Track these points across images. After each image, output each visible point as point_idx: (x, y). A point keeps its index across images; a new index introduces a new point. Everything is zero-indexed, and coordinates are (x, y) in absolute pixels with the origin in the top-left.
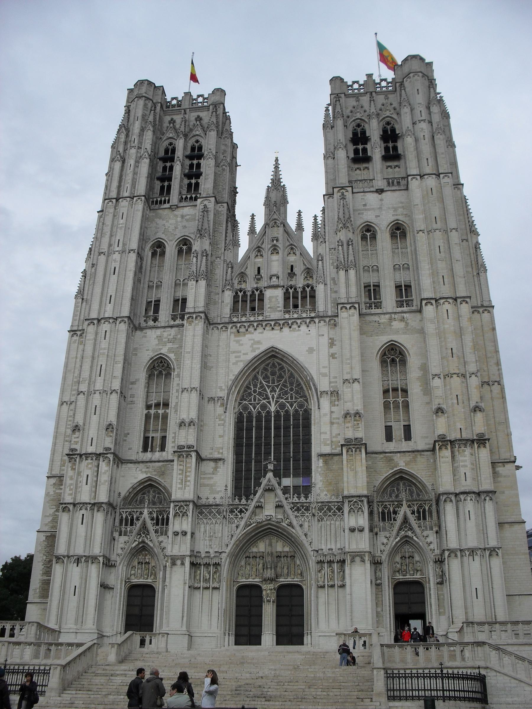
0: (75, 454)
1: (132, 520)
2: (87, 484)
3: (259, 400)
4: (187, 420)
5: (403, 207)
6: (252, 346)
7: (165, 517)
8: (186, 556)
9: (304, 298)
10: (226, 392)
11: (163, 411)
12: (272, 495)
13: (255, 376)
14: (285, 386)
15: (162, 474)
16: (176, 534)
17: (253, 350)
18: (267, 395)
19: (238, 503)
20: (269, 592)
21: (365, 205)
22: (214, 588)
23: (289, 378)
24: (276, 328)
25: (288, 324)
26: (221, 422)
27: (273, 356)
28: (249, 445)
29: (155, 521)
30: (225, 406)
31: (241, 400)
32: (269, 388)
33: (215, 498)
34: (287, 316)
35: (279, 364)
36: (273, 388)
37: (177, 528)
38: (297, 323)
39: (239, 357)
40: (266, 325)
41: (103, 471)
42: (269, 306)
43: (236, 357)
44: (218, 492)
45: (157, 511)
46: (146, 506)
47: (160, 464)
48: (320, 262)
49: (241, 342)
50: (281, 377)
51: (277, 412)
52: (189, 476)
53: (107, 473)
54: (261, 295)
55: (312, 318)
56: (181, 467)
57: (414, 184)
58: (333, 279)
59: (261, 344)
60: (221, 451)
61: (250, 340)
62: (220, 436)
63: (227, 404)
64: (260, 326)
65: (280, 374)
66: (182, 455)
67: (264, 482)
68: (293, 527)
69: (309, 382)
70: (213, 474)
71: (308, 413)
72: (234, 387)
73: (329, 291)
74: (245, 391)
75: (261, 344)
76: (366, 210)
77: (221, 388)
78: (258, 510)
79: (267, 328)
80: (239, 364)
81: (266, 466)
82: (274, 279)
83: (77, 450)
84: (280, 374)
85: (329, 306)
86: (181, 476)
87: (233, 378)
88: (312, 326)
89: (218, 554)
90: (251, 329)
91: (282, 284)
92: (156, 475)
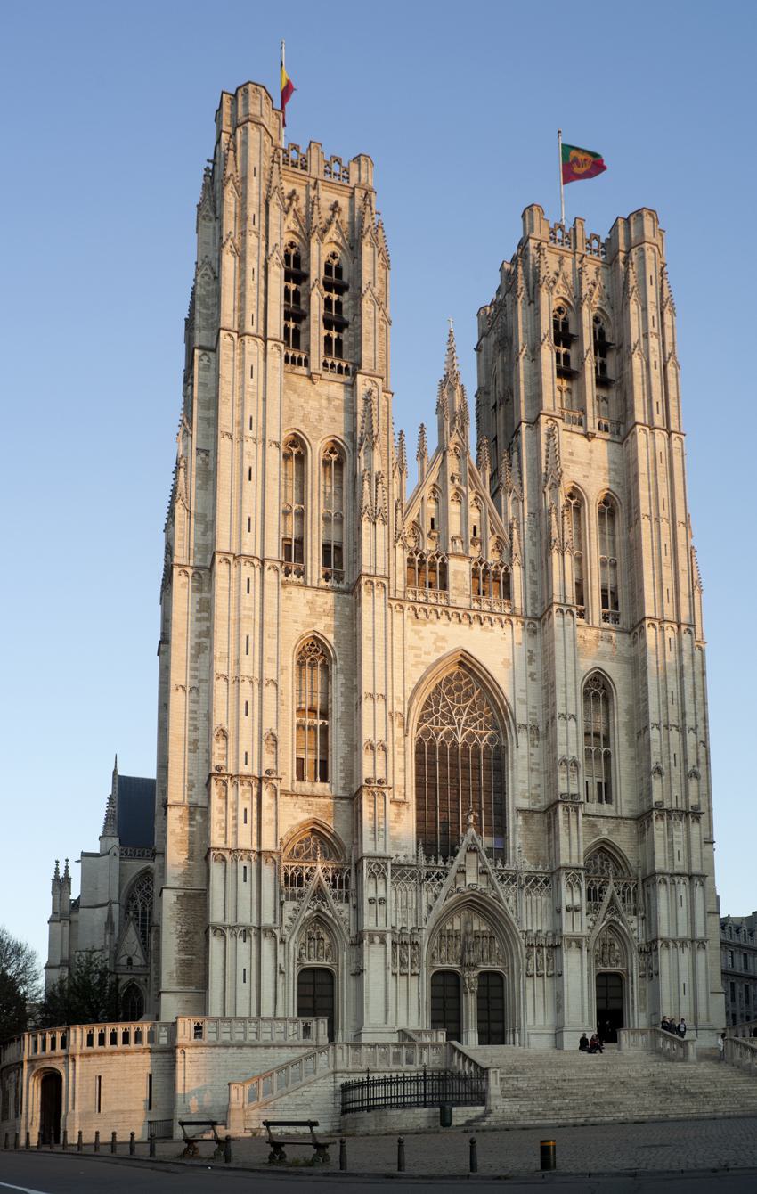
1: (300, 878)
6: (434, 643)
7: (344, 877)
10: (406, 706)
12: (474, 856)
13: (436, 687)
17: (437, 650)
19: (435, 865)
21: (571, 454)
29: (331, 883)
30: (405, 725)
34: (476, 606)
42: (454, 585)
43: (416, 656)
48: (515, 532)
49: (421, 635)
54: (444, 567)
55: (508, 615)
57: (641, 437)
58: (532, 562)
59: (446, 642)
61: (432, 633)
63: (408, 725)
67: (466, 840)
70: (396, 822)
72: (415, 702)
73: (528, 580)
74: (425, 708)
75: (446, 642)
76: (573, 462)
78: (460, 876)
80: (420, 666)
82: (458, 543)
85: (529, 601)
87: (413, 687)
91: (471, 555)
92: (321, 816)
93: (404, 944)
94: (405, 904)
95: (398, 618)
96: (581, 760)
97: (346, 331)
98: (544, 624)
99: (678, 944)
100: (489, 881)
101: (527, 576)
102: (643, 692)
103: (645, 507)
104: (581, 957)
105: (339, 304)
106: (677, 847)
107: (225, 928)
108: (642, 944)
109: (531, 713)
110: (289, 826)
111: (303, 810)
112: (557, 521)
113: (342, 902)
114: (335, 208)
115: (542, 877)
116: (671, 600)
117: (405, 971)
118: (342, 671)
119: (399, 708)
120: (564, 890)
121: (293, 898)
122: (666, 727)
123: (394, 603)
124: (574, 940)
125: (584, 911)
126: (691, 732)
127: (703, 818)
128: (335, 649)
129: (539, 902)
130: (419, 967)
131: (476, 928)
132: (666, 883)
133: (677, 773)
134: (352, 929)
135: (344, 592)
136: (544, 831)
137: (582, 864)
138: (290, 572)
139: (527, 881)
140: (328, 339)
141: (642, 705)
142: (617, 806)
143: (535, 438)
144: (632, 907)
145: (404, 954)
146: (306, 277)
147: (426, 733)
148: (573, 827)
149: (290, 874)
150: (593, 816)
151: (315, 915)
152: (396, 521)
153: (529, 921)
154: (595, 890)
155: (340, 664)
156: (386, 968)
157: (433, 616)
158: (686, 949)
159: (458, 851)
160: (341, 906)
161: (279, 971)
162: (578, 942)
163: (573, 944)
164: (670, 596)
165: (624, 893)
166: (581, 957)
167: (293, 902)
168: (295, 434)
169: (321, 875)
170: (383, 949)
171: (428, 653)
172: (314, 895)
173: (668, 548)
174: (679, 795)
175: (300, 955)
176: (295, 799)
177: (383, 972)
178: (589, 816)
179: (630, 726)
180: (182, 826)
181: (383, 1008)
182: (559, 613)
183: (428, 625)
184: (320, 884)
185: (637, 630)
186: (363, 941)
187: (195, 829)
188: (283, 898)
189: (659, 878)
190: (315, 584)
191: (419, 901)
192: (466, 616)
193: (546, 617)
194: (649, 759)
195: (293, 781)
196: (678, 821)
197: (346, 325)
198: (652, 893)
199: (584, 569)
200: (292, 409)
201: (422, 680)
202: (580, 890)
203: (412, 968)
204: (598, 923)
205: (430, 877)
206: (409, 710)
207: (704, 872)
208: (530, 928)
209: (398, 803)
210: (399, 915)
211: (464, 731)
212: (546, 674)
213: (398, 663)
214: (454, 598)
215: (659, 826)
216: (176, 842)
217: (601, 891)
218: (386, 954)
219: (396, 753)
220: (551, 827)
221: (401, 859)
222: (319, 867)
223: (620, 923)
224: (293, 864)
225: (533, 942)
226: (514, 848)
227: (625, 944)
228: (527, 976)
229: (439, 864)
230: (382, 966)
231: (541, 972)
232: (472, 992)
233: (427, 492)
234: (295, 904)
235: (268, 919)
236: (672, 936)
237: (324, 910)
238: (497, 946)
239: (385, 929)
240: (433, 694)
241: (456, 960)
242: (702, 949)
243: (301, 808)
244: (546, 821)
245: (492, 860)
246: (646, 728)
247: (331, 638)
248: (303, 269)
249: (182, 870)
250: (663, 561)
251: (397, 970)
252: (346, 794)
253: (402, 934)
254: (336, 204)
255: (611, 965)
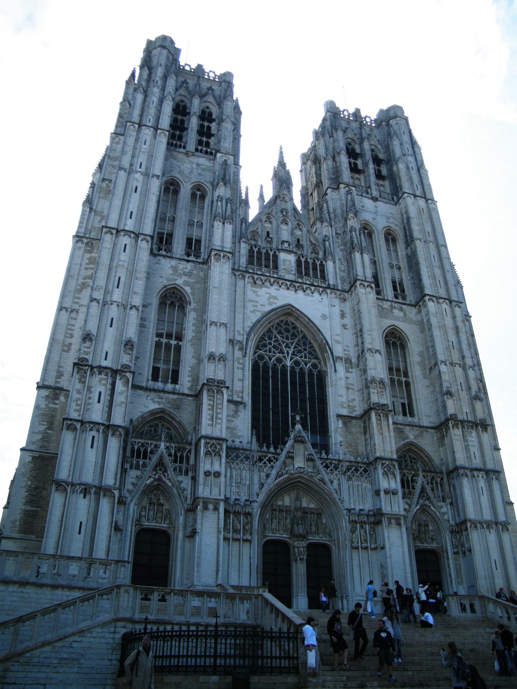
0: (86, 365)
1: (145, 452)
2: (99, 401)
3: (274, 352)
4: (217, 355)
5: (393, 218)
6: (269, 299)
7: (185, 455)
8: (221, 500)
9: (315, 269)
10: (245, 337)
11: (175, 342)
13: (269, 329)
14: (299, 345)
15: (178, 407)
16: (207, 474)
17: (270, 304)
18: (281, 350)
19: (266, 450)
20: (302, 549)
22: (244, 540)
23: (302, 338)
24: (291, 288)
25: (303, 288)
26: (239, 366)
27: (289, 314)
28: (266, 395)
30: (243, 349)
31: (256, 349)
32: (283, 343)
33: (241, 442)
35: (292, 324)
36: (287, 344)
37: (208, 467)
38: (310, 289)
39: (257, 306)
40: (282, 284)
41: (119, 391)
44: (239, 437)
45: (175, 447)
46: (163, 439)
47: (176, 397)
48: (327, 243)
49: (258, 293)
50: (294, 336)
51: (292, 368)
52: (220, 414)
53: (124, 394)
56: (211, 403)
57: (410, 201)
58: (340, 259)
59: (278, 299)
60: (241, 395)
61: (266, 293)
62: (239, 380)
63: (246, 349)
64: (276, 283)
65: (294, 333)
66: (212, 389)
68: (325, 484)
69: (325, 346)
70: (234, 417)
71: (322, 376)
73: (338, 269)
74: (260, 341)
75: (278, 299)
77: (239, 332)
79: (283, 287)
81: (293, 418)
83: (87, 360)
84: (294, 333)
85: (339, 281)
86: (211, 412)
87: (251, 325)
88: (324, 296)
89: (248, 503)
90: (267, 284)
93: (237, 514)
94: (239, 480)
95: (240, 283)
96: (387, 381)
97: (212, 138)
98: (351, 295)
99: (485, 526)
100: (314, 467)
101: (337, 267)
102: (431, 341)
103: (416, 234)
104: (401, 533)
105: (209, 128)
106: (472, 450)
107: (68, 485)
108: (452, 526)
109: (344, 350)
110: (141, 412)
111: (154, 402)
112: (356, 236)
113: (181, 474)
114: (210, 89)
115: (361, 467)
116: (442, 286)
117: (237, 536)
118: (194, 310)
119: (238, 338)
120: (381, 477)
121: (137, 468)
122: (451, 364)
123: (237, 273)
124: (393, 518)
125: (400, 494)
126: (471, 369)
127: (489, 428)
128: (191, 296)
129: (360, 487)
130: (251, 534)
131: (304, 505)
132: (467, 476)
133: (464, 395)
134: (189, 497)
135: (200, 263)
136: (361, 433)
137: (395, 457)
138: (161, 250)
139: (348, 469)
140: (200, 143)
141: (430, 350)
142: (419, 419)
143: (338, 197)
144: (441, 495)
145: (236, 522)
146: (189, 114)
147: (261, 357)
148: (385, 429)
149: (136, 448)
150: (401, 424)
151: (156, 483)
152: (241, 228)
153: (352, 502)
154: (408, 480)
155: (193, 306)
156: (219, 532)
157: (267, 284)
158: (492, 530)
159: (287, 442)
160: (180, 478)
161: (117, 528)
162: (397, 520)
163: (393, 521)
164: (442, 285)
165: (432, 484)
166: (401, 533)
167: (136, 471)
168: (173, 179)
169: (165, 451)
170: (216, 516)
171: (264, 305)
172: (156, 466)
173: (436, 258)
174: (468, 411)
175: (140, 516)
176: (148, 393)
177: (216, 535)
178: (397, 424)
179: (422, 364)
180: (47, 403)
181: (214, 568)
182: (362, 286)
183: (263, 289)
184: (161, 458)
185: (421, 304)
186: (197, 507)
187: (57, 406)
188: (127, 466)
189: (461, 471)
190: (178, 256)
191: (251, 478)
192: (292, 285)
193: (353, 289)
194: (441, 385)
195: (148, 380)
196: (470, 430)
197: (213, 135)
198: (456, 483)
199: (378, 267)
200: (171, 167)
201: (258, 321)
202: (395, 477)
203: (244, 534)
204: (413, 506)
205: (263, 460)
206: (247, 340)
207: (497, 469)
208: (353, 507)
209: (237, 403)
210: (234, 489)
211: (291, 359)
212: (356, 324)
213: (239, 309)
214: (283, 274)
215: (456, 434)
216: (39, 415)
217: (413, 481)
218: (219, 519)
219: (235, 368)
220: (366, 430)
221: (237, 444)
222: (163, 445)
223: (432, 507)
224: (140, 441)
225: (356, 518)
226: (335, 444)
227: (437, 524)
228: (352, 548)
229: (270, 451)
230: (215, 531)
231: (364, 545)
232: (302, 559)
233: (264, 218)
234: (138, 473)
235: (109, 480)
236: (478, 518)
237: (164, 479)
238: (324, 521)
239: (219, 498)
240: (267, 332)
241: (285, 531)
242: (506, 531)
243: (152, 400)
244: (362, 425)
245: (317, 450)
246: (436, 364)
247: (188, 289)
248: (188, 111)
249: (40, 436)
250: (434, 264)
251: (230, 535)
252: (193, 393)
253: (235, 504)
254: (211, 87)
255: (427, 543)
